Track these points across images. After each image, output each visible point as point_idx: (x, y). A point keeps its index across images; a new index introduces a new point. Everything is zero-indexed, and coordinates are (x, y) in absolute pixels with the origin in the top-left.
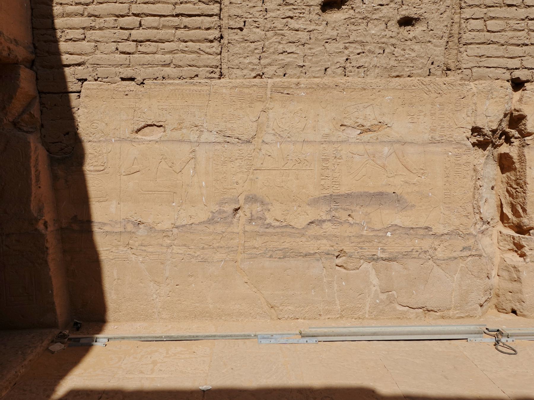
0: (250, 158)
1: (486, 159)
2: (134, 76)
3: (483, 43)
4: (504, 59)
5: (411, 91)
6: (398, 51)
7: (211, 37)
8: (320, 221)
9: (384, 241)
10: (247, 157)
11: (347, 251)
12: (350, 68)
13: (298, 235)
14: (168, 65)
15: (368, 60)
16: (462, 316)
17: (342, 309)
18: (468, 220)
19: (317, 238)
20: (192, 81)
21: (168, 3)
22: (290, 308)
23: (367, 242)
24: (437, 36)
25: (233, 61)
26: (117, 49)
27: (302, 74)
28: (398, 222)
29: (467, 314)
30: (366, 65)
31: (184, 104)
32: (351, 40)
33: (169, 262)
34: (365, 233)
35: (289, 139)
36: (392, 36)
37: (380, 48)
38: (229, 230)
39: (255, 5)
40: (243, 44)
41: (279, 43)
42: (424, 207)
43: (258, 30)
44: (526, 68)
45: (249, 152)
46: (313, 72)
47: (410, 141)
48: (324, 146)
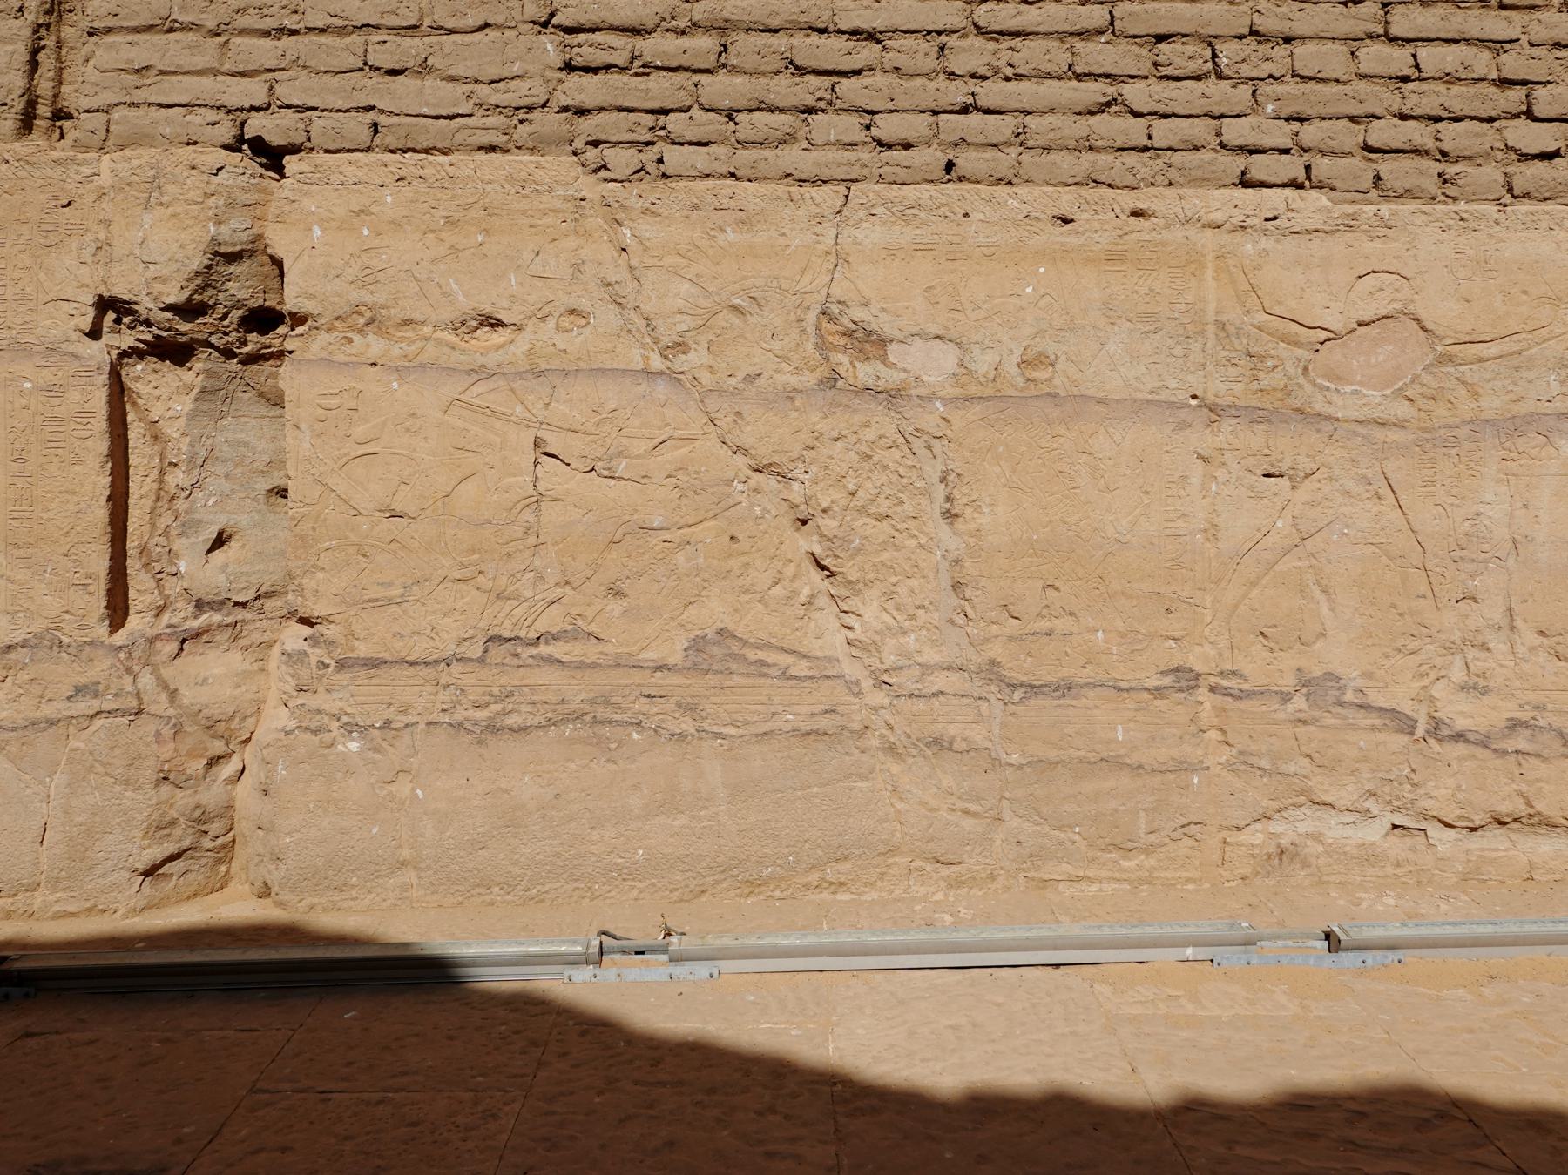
1: (196, 400)
3: (149, 29)
4: (220, 78)
16: (71, 909)
18: (87, 597)
29: (88, 904)
44: (288, 107)
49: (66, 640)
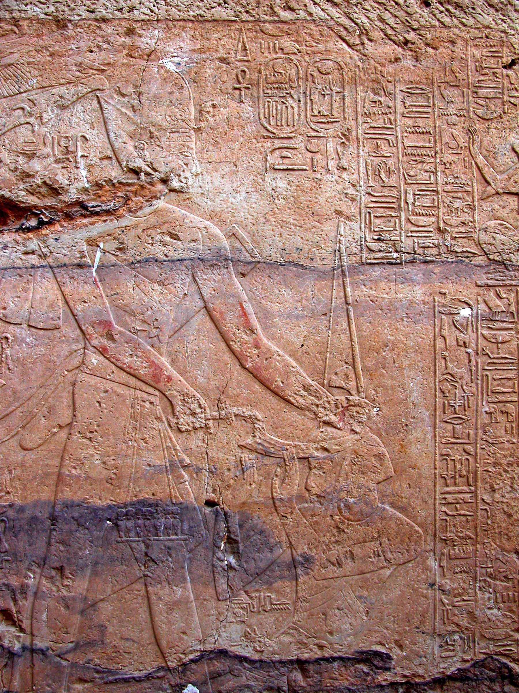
28: (230, 637)
42: (349, 565)
47: (276, 255)
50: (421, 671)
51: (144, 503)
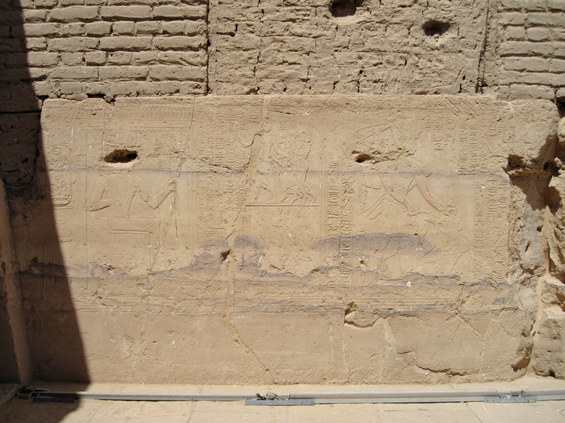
0: (242, 192)
2: (103, 92)
5: (436, 111)
6: (422, 62)
7: (195, 45)
8: (326, 268)
9: (403, 293)
10: (238, 191)
11: (357, 304)
12: (365, 82)
13: (299, 285)
14: (144, 79)
15: (386, 72)
16: (491, 379)
17: (350, 372)
19: (322, 288)
20: (172, 97)
21: (145, 4)
22: (288, 370)
23: (382, 293)
24: (470, 44)
25: (222, 73)
26: (84, 60)
27: (306, 89)
28: (419, 269)
29: (497, 377)
30: (384, 79)
31: (162, 126)
32: (367, 47)
33: (145, 315)
34: (380, 283)
35: (289, 169)
36: (416, 44)
37: (401, 58)
38: (216, 278)
39: (249, 5)
40: (235, 52)
41: (279, 51)
43: (252, 35)
45: (240, 184)
46: (319, 86)
48: (332, 177)
49: (493, 282)
50: (468, 281)
51: (400, 233)
